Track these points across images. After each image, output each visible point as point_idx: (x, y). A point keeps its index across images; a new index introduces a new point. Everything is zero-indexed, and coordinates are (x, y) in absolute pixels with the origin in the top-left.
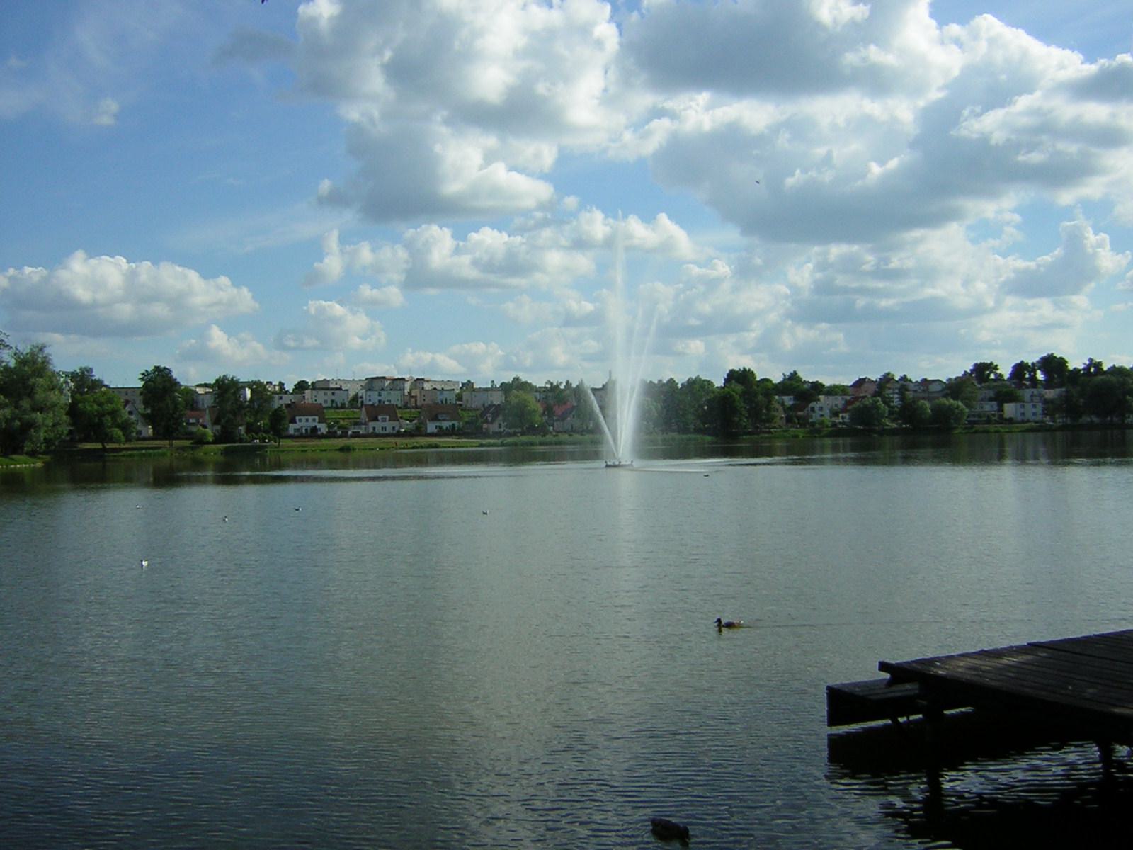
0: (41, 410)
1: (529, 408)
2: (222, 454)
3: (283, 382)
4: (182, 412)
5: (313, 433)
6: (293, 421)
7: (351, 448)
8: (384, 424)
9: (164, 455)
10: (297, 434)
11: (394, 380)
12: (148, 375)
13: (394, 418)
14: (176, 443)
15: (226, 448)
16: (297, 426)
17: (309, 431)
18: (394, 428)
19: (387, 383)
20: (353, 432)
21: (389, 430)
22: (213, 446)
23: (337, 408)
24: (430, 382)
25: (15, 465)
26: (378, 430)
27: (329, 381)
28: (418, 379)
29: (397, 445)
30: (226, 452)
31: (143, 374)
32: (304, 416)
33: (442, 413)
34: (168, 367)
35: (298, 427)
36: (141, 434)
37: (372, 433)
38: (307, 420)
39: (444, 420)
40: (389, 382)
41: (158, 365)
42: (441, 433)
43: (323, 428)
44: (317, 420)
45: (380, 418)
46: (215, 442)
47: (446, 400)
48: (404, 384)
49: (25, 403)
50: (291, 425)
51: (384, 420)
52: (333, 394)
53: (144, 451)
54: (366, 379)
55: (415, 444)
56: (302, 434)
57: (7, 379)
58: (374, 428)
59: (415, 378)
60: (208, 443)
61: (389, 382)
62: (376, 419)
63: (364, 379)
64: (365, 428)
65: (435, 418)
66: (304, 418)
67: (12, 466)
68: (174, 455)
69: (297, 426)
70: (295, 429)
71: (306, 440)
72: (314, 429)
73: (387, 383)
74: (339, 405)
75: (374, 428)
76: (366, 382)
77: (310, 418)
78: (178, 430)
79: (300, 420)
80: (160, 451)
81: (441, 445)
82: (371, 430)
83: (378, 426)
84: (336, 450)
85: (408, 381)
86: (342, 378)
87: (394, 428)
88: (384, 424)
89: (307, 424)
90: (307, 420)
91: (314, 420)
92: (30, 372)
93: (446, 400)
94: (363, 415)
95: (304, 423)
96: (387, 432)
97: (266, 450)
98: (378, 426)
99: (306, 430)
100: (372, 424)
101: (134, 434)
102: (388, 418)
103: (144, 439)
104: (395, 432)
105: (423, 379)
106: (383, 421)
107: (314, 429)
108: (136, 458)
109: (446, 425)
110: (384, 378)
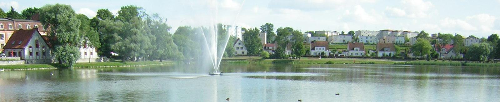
0: (135, 42)
1: (424, 46)
2: (272, 63)
3: (344, 31)
4: (256, 44)
5: (322, 55)
6: (313, 49)
7: (332, 62)
8: (357, 52)
9: (245, 63)
10: (315, 55)
11: (393, 31)
12: (264, 27)
13: (362, 49)
14: (253, 57)
15: (275, 60)
16: (315, 51)
17: (320, 54)
18: (361, 54)
19: (389, 33)
20: (341, 55)
21: (359, 55)
22: (269, 59)
23: (345, 44)
24: (411, 33)
25: (123, 65)
26: (354, 55)
27: (361, 31)
28: (405, 32)
29: (354, 62)
30: (274, 62)
31: (261, 27)
32: (321, 47)
33: (385, 48)
34: (272, 24)
35: (316, 52)
36: (244, 53)
37: (351, 56)
38: (320, 49)
39: (387, 51)
40: (390, 32)
41: (267, 23)
42: (383, 57)
43: (327, 53)
44: (325, 49)
45: (355, 49)
46: (270, 58)
47: (399, 42)
48: (397, 33)
49: (127, 40)
50: (312, 51)
51: (357, 50)
52: (344, 37)
53: (237, 61)
54: (380, 31)
55: (362, 62)
56: (317, 55)
57: (123, 29)
58: (352, 54)
59: (404, 31)
60: (267, 58)
61: (390, 32)
62: (353, 49)
63: (379, 31)
64: (348, 53)
65: (382, 50)
66: (318, 48)
67: (122, 66)
68: (251, 63)
69: (315, 51)
70: (314, 53)
71: (387, 59)
72: (323, 53)
73: (389, 33)
74: (346, 42)
75: (352, 54)
76: (379, 32)
77: (322, 48)
78: (253, 52)
79: (317, 49)
80: (244, 61)
81: (375, 63)
82: (350, 54)
83: (354, 53)
84: (326, 63)
85: (400, 32)
86: (367, 30)
87: (361, 54)
88: (357, 52)
89: (320, 51)
90: (320, 49)
91: (323, 49)
92: (132, 26)
93: (399, 42)
94: (348, 47)
95: (318, 50)
96: (358, 56)
97: (293, 62)
98: (354, 53)
99: (319, 53)
100: (351, 52)
101: (234, 53)
102: (359, 49)
103: (239, 55)
104: (361, 56)
105: (407, 32)
106: (356, 50)
107: (323, 53)
108: (233, 64)
109: (387, 53)
110: (388, 30)
